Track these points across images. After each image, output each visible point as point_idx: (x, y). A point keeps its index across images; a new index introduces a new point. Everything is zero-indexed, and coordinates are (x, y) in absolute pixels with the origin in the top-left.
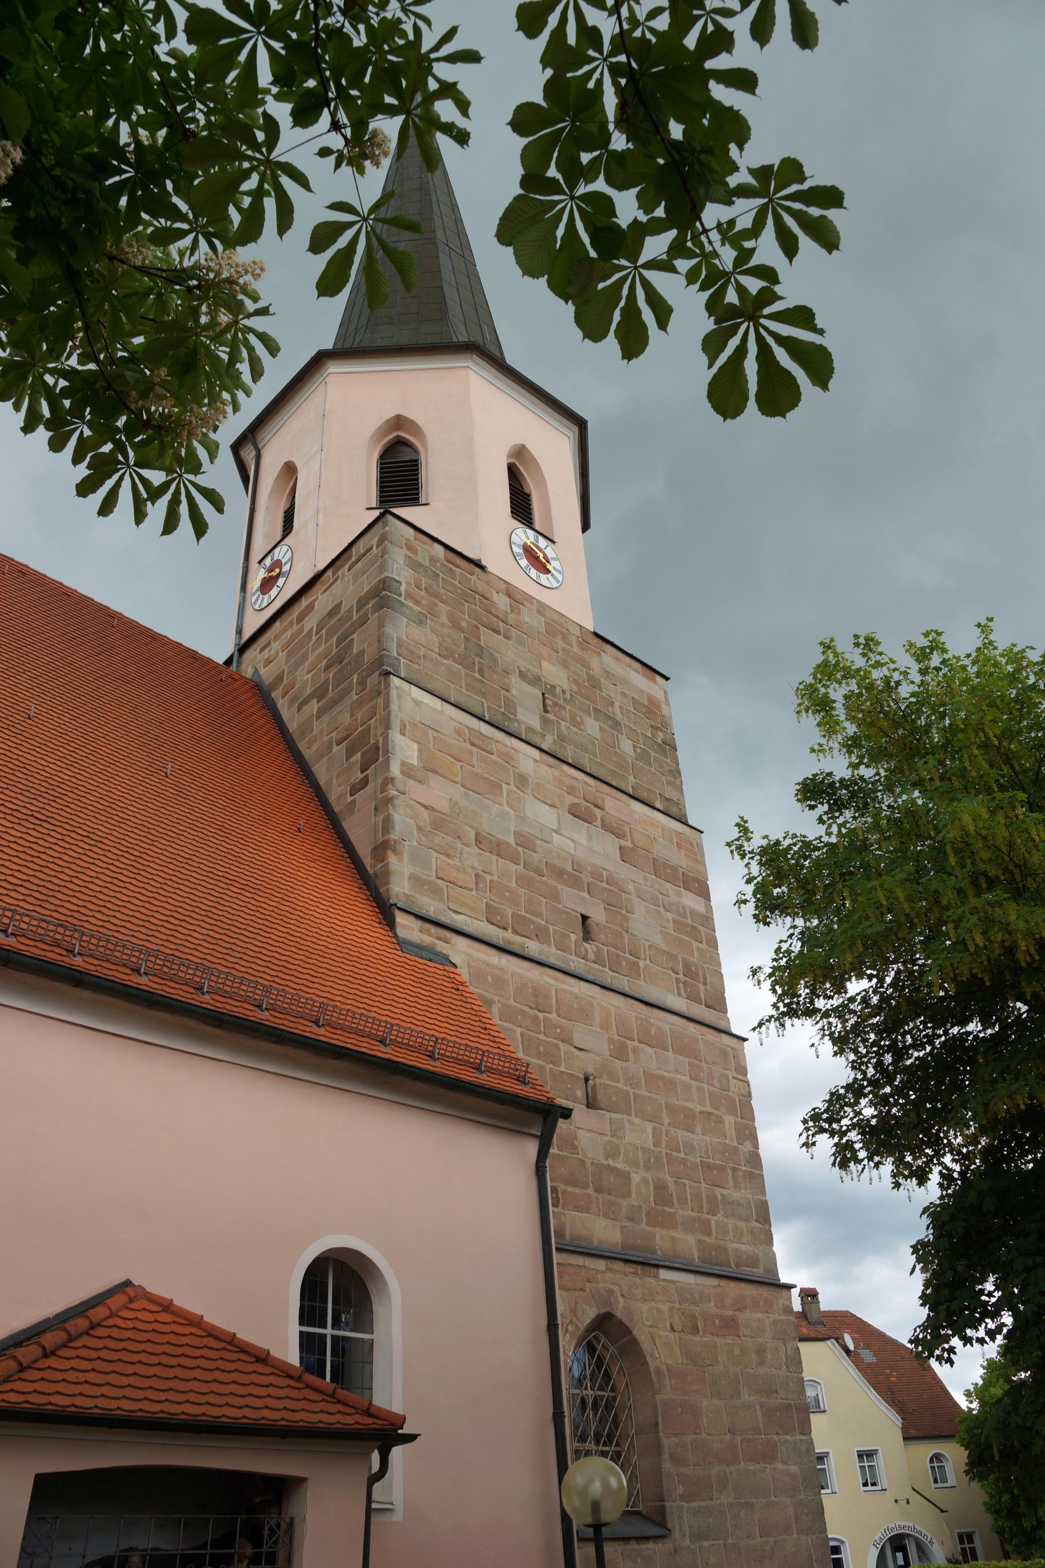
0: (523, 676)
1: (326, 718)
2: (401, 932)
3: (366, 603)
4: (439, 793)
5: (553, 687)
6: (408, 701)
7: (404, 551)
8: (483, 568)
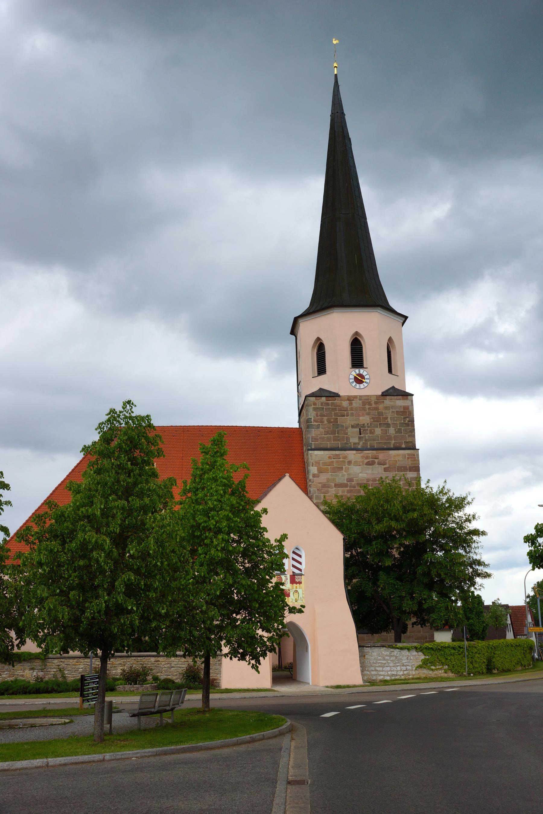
0: (353, 427)
4: (323, 478)
5: (364, 424)
6: (315, 456)
7: (313, 406)
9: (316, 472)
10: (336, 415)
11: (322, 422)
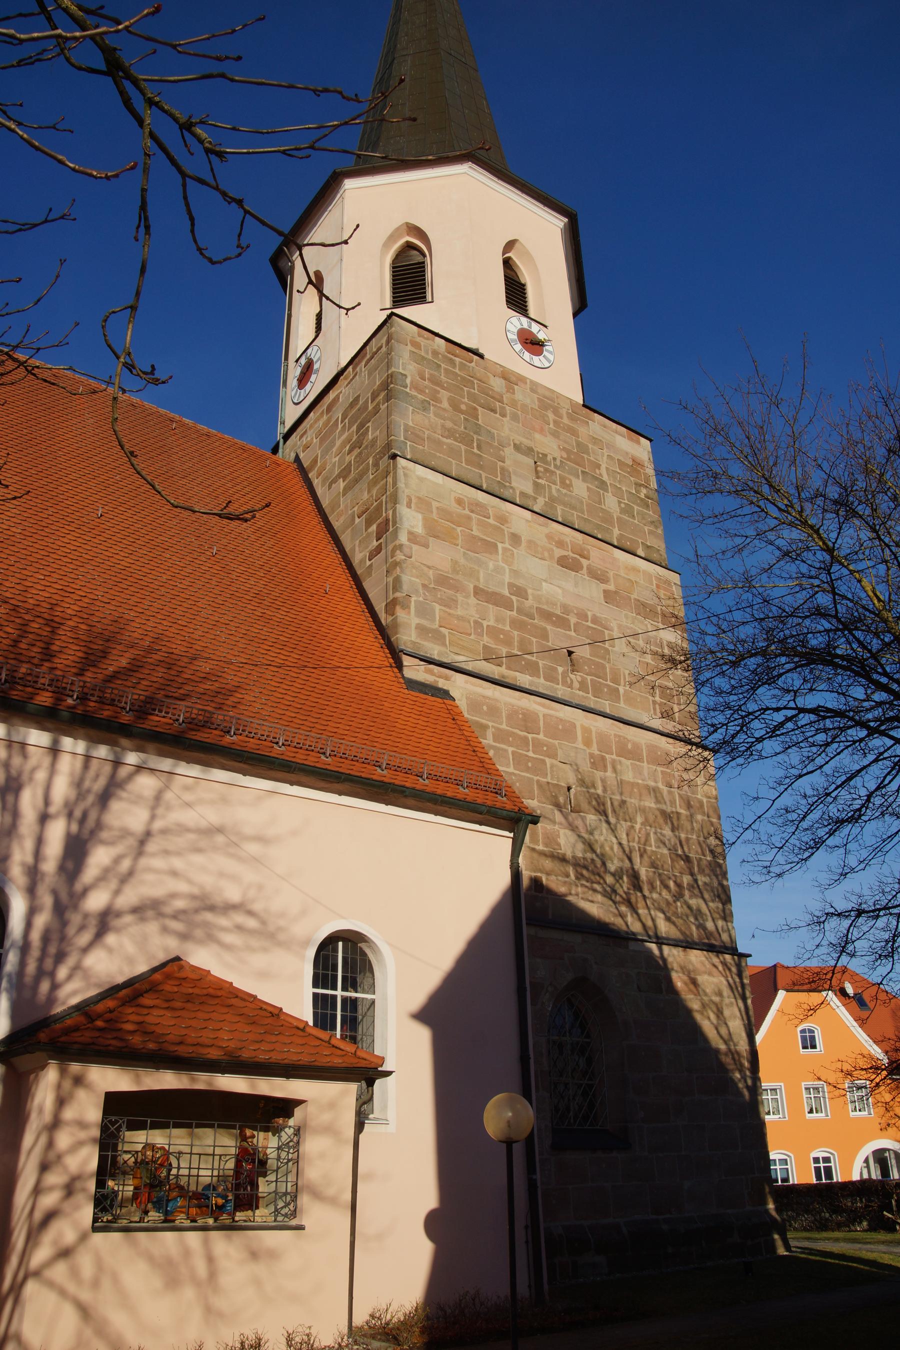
0: (517, 447)
1: (349, 495)
2: (408, 673)
3: (378, 395)
4: (440, 556)
5: (545, 455)
6: (414, 478)
7: (409, 347)
8: (481, 356)
9: (419, 529)
10: (472, 397)
11: (438, 400)
